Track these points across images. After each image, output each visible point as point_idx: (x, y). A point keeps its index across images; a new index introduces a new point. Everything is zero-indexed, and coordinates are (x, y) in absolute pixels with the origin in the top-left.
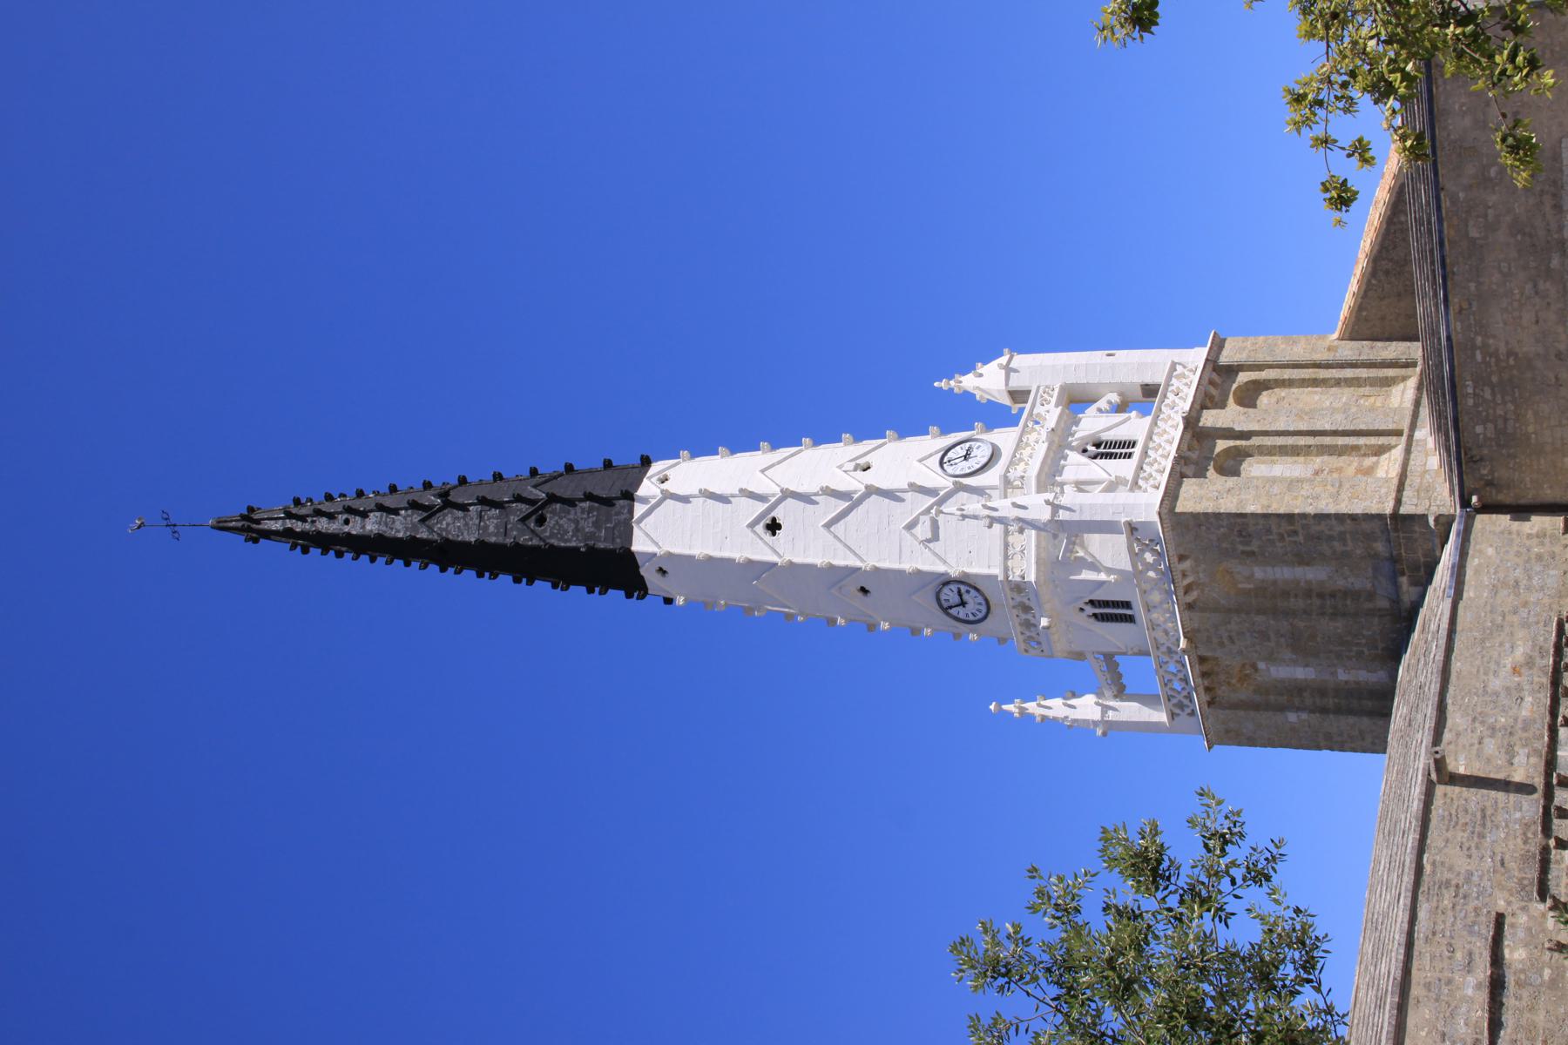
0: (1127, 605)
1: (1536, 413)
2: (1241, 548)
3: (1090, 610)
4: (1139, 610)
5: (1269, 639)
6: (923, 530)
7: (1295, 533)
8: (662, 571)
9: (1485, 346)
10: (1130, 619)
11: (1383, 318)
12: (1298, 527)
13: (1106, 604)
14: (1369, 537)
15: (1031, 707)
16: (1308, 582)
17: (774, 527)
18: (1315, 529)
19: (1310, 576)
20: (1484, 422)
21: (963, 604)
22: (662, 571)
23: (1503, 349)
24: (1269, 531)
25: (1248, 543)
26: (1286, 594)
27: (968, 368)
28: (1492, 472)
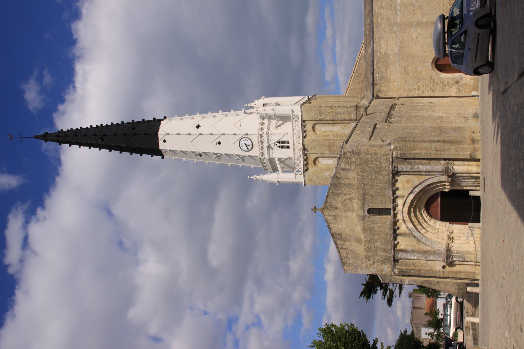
0: (288, 142)
1: (390, 71)
2: (319, 117)
3: (278, 145)
4: (291, 145)
5: (322, 147)
6: (238, 125)
7: (333, 112)
8: (165, 141)
9: (379, 52)
10: (288, 147)
11: (355, 89)
12: (334, 110)
13: (283, 142)
14: (350, 113)
15: (258, 177)
16: (334, 132)
17: (198, 127)
18: (338, 111)
19: (335, 129)
20: (378, 73)
21: (246, 145)
22: (165, 141)
23: (383, 53)
24: (326, 112)
25: (320, 116)
26: (328, 136)
27: (253, 101)
28: (379, 88)
